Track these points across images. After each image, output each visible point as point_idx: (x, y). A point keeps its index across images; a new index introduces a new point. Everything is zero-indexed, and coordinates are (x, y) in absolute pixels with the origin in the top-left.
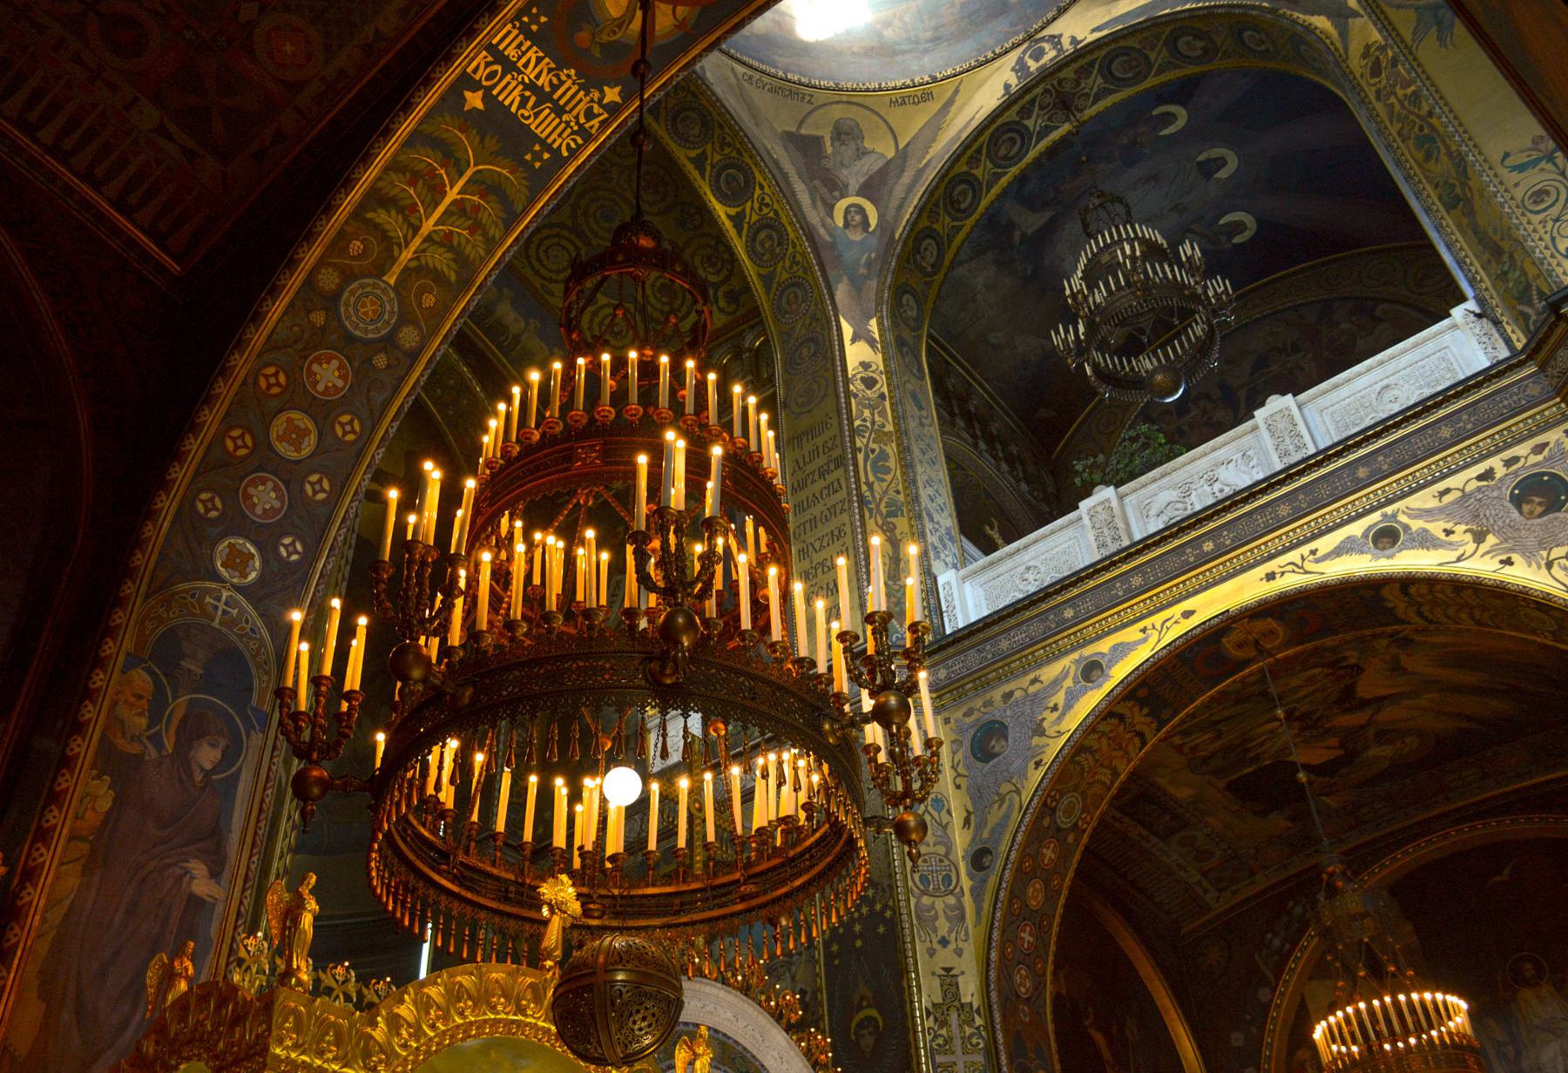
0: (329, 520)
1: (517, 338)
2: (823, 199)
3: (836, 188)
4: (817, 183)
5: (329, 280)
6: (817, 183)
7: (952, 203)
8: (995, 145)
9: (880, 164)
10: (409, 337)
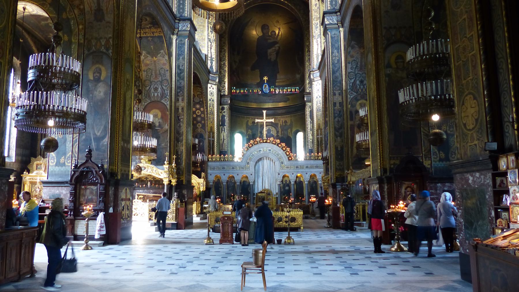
10: (201, 100)
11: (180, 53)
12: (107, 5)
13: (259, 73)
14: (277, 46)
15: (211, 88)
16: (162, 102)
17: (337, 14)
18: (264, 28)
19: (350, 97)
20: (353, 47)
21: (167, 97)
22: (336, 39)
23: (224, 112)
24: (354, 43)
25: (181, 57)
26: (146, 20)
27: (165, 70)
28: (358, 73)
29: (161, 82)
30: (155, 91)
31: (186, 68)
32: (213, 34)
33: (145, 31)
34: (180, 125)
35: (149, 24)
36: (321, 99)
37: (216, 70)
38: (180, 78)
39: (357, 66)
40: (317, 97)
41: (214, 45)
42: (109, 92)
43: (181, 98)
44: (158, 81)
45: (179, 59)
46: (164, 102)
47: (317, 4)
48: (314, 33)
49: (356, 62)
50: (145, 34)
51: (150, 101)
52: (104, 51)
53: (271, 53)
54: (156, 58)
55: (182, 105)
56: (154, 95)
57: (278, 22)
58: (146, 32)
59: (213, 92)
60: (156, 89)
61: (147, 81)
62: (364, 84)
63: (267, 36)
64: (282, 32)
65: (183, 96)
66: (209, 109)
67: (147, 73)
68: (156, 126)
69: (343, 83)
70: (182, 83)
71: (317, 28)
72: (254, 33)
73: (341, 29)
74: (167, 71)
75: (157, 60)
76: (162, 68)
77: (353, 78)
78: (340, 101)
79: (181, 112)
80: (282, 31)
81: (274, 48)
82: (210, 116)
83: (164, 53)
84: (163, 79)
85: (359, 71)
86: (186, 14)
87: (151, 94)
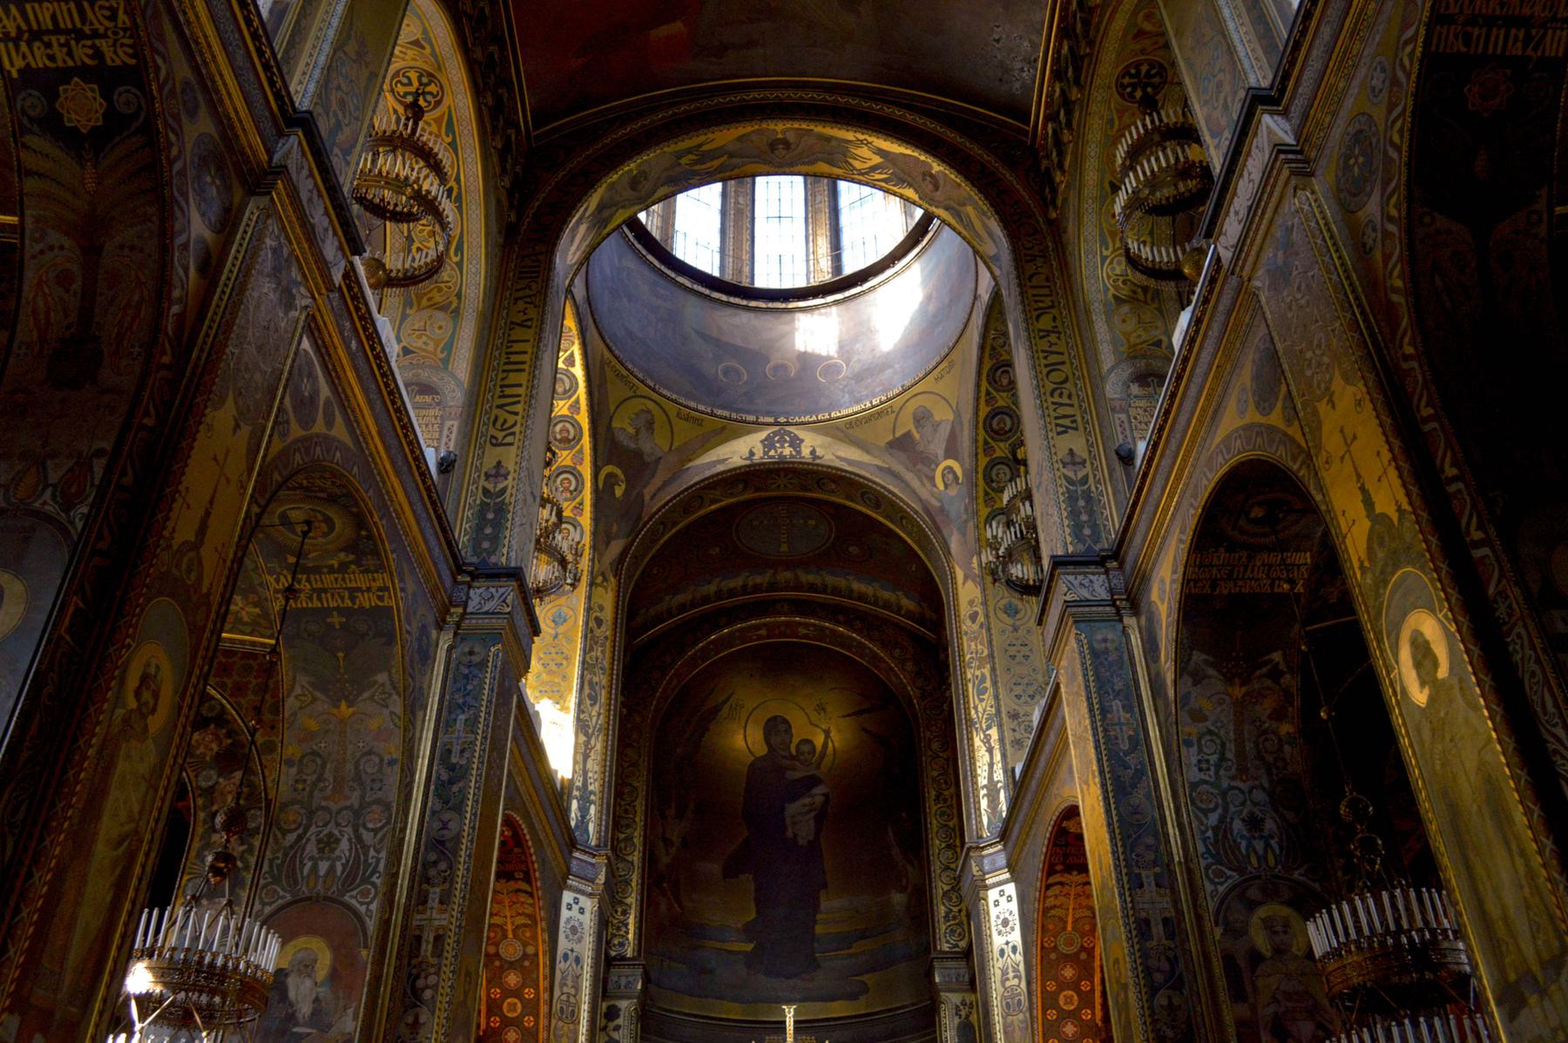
0: (537, 1030)
1: (874, 596)
2: (927, 476)
3: (931, 462)
4: (919, 466)
5: (492, 950)
6: (919, 466)
7: (996, 433)
9: (949, 428)
10: (530, 950)
11: (461, 701)
12: (129, 319)
13: (752, 887)
14: (819, 790)
15: (575, 907)
16: (341, 903)
17: (1108, 565)
18: (776, 728)
19: (1216, 890)
20: (1198, 679)
21: (374, 879)
22: (1113, 657)
23: (617, 1028)
24: (1206, 661)
25: (462, 717)
26: (331, 527)
27: (382, 760)
28: (1233, 788)
29: (357, 813)
30: (321, 850)
31: (476, 760)
32: (597, 708)
33: (319, 585)
34: (417, 1017)
35: (341, 550)
36: (1019, 958)
37: (599, 839)
38: (446, 802)
39: (1222, 758)
40: (1002, 952)
41: (598, 745)
42: (11, 703)
43: (438, 890)
44: (346, 808)
45: (450, 724)
46: (353, 902)
47: (976, 614)
48: (973, 712)
49: (1218, 741)
50: (320, 599)
51: (289, 897)
52: (51, 508)
53: (799, 817)
54: (350, 704)
55: (436, 923)
56: (315, 869)
57: (821, 708)
58: (325, 591)
59: (581, 924)
60: (328, 844)
61: (296, 807)
62: (1266, 833)
63: (784, 757)
64: (836, 745)
65: (449, 879)
66: (557, 993)
67: (300, 772)
68: (299, 1016)
69: (1171, 831)
70: (451, 825)
71: (982, 692)
72: (739, 741)
73: (1130, 621)
74: (391, 763)
75: (354, 714)
76: (370, 753)
77: (1212, 806)
78: (1168, 915)
79: (429, 954)
80: (837, 740)
81: (807, 800)
82: (560, 1024)
83: (388, 683)
84: (367, 799)
85: (1233, 778)
86: (502, 559)
87: (303, 865)
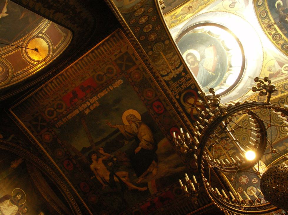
2: (282, 75)
6: (278, 76)
8: (276, 40)
